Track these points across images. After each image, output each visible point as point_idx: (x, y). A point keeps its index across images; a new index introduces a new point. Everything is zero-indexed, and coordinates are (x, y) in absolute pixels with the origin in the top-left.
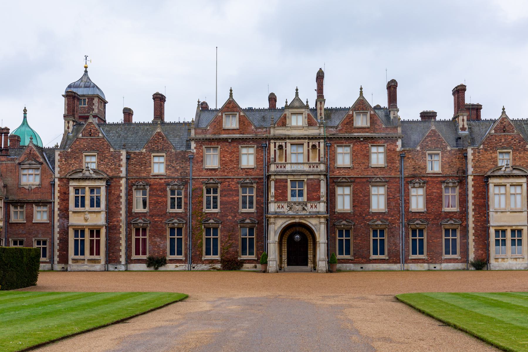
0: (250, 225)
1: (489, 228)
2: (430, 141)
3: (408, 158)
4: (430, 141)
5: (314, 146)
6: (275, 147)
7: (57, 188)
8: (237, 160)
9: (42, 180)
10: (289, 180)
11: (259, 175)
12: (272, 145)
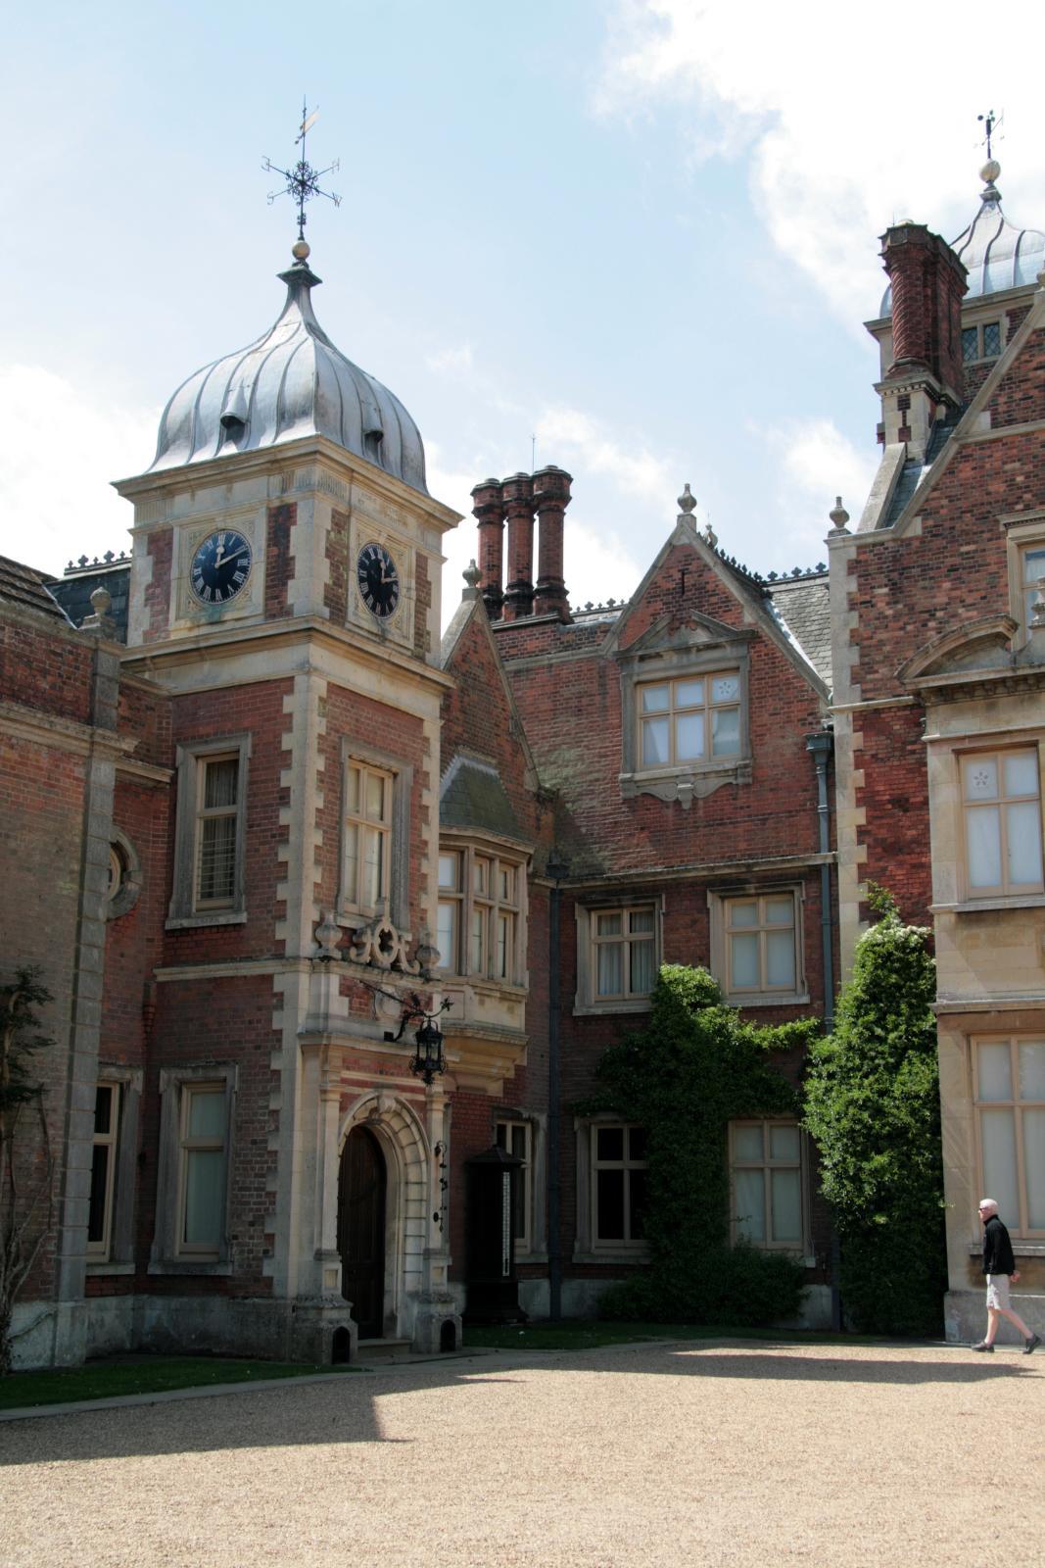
7: (850, 777)
9: (754, 736)
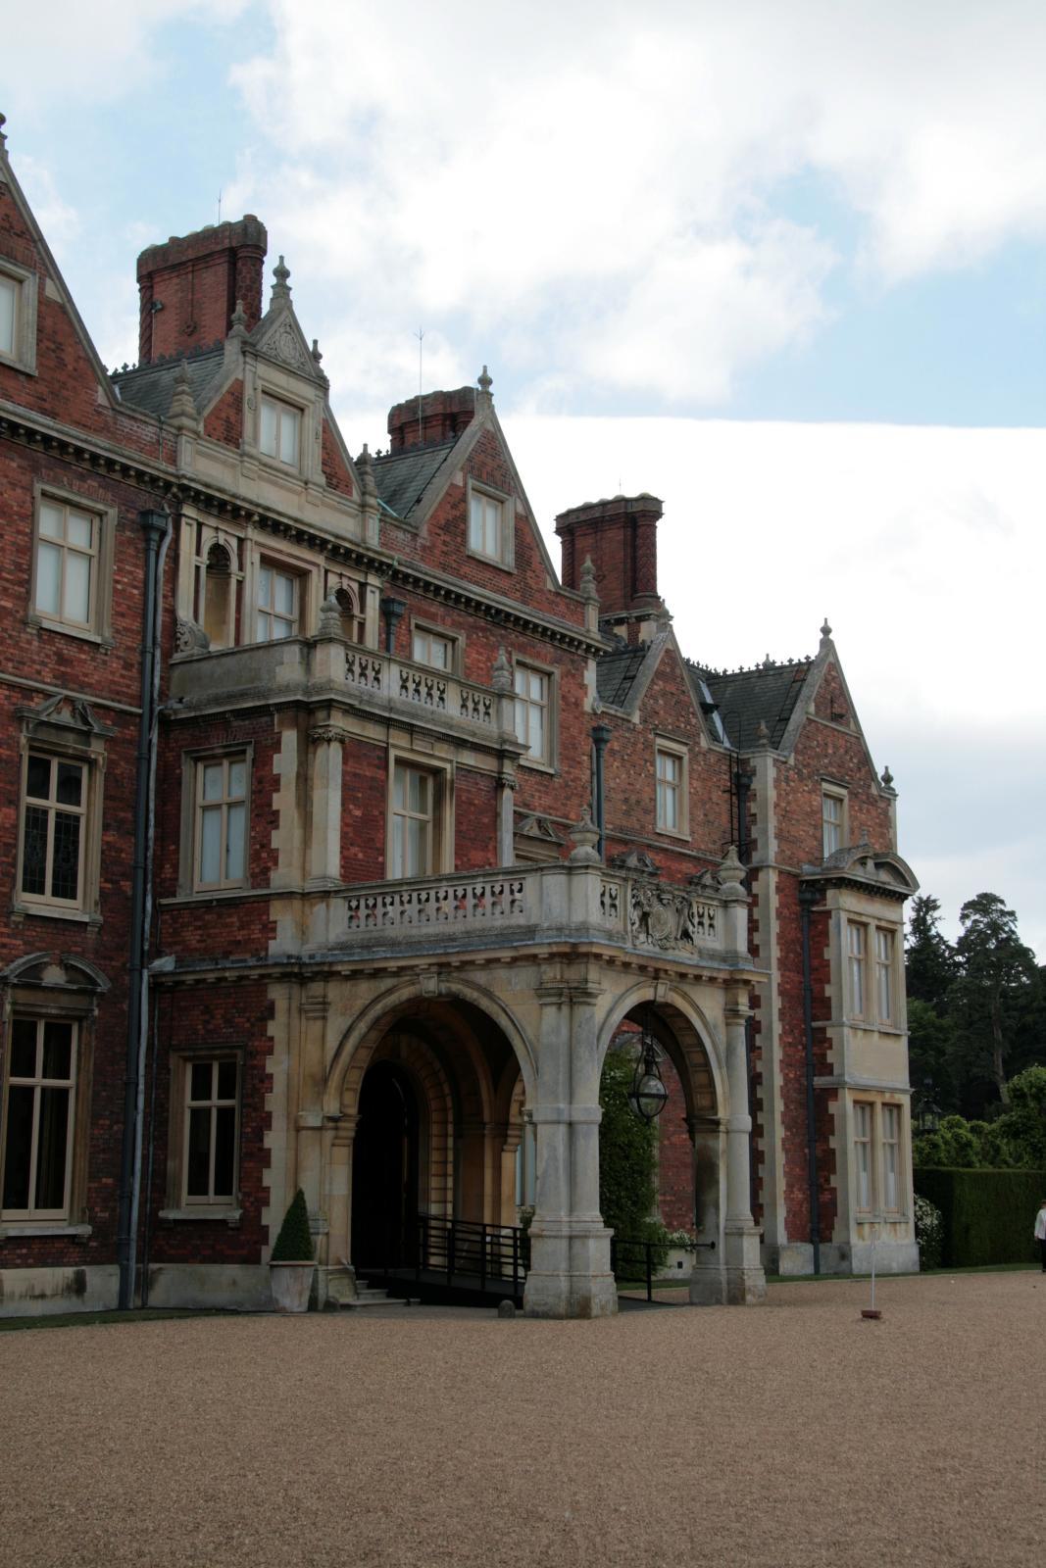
0: (65, 1001)
1: (832, 1093)
2: (664, 694)
3: (612, 752)
4: (664, 694)
5: (342, 595)
6: (198, 553)
8: (19, 567)
10: (393, 753)
11: (117, 695)
12: (187, 534)
